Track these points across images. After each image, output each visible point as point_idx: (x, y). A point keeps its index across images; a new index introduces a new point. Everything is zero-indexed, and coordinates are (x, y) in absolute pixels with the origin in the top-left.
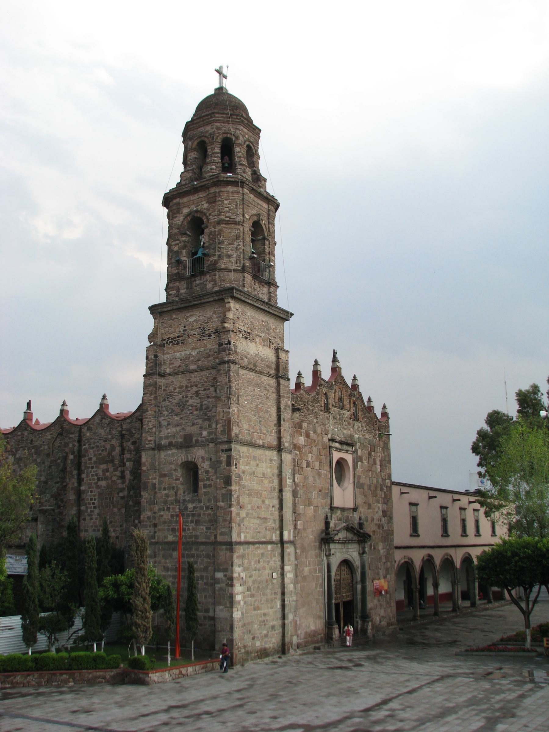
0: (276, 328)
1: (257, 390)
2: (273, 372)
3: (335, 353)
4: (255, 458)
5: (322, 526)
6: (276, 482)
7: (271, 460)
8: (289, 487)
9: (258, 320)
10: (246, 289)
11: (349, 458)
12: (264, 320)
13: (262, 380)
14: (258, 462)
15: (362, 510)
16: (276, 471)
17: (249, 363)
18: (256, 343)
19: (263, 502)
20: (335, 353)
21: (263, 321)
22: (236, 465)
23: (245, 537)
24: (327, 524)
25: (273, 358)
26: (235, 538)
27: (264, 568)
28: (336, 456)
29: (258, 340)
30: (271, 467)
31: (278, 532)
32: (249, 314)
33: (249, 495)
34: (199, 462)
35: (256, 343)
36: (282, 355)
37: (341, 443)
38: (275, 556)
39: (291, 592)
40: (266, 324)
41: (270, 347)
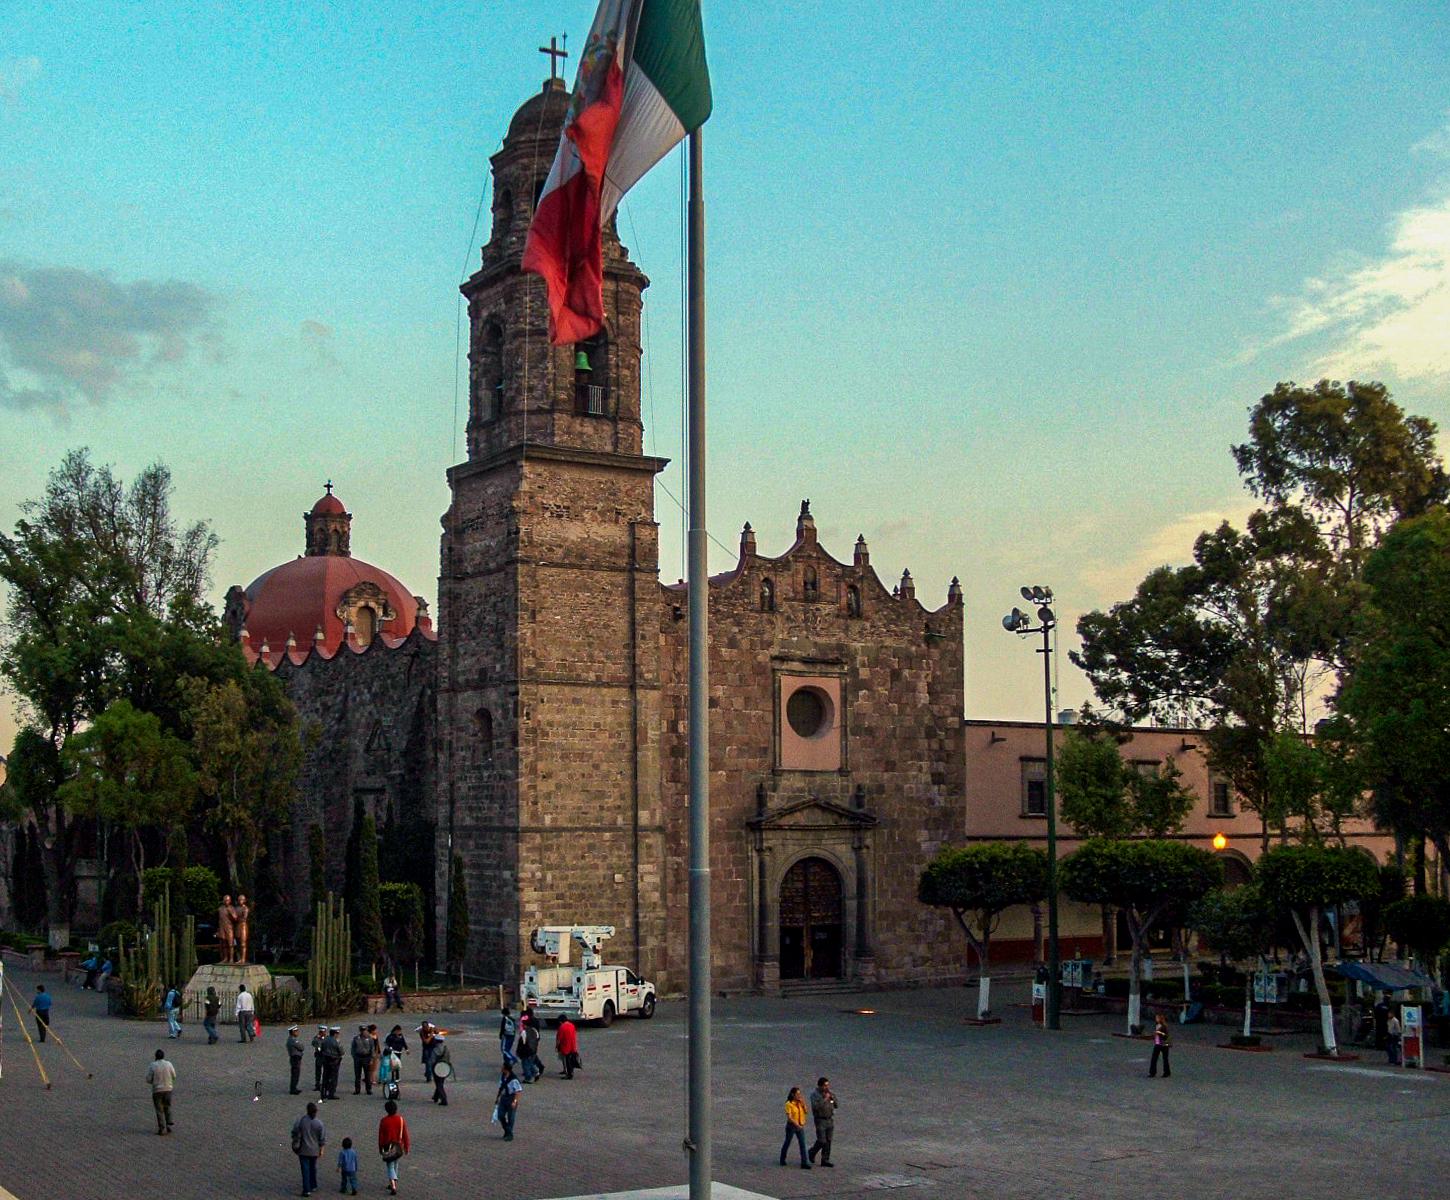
0: (633, 489)
1: (584, 596)
2: (623, 562)
3: (805, 505)
4: (576, 701)
5: (749, 801)
6: (625, 737)
7: (615, 702)
8: (653, 742)
9: (590, 484)
10: (557, 439)
11: (832, 686)
12: (604, 480)
13: (596, 578)
14: (583, 706)
15: (865, 777)
16: (625, 719)
17: (566, 556)
18: (583, 520)
19: (596, 767)
20: (805, 505)
21: (600, 483)
22: (528, 714)
23: (554, 820)
24: (761, 798)
25: (626, 539)
26: (525, 819)
27: (596, 867)
28: (789, 685)
29: (587, 515)
30: (614, 713)
31: (630, 814)
32: (566, 477)
33: (562, 757)
34: (492, 708)
35: (583, 520)
36: (644, 533)
37: (805, 661)
38: (619, 849)
39: (655, 903)
40: (609, 484)
41: (617, 522)
